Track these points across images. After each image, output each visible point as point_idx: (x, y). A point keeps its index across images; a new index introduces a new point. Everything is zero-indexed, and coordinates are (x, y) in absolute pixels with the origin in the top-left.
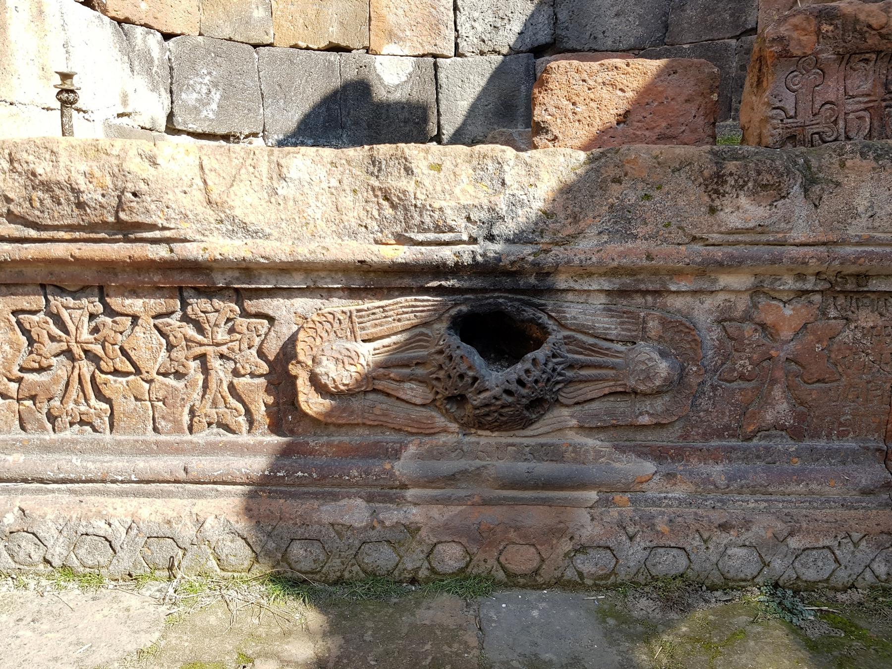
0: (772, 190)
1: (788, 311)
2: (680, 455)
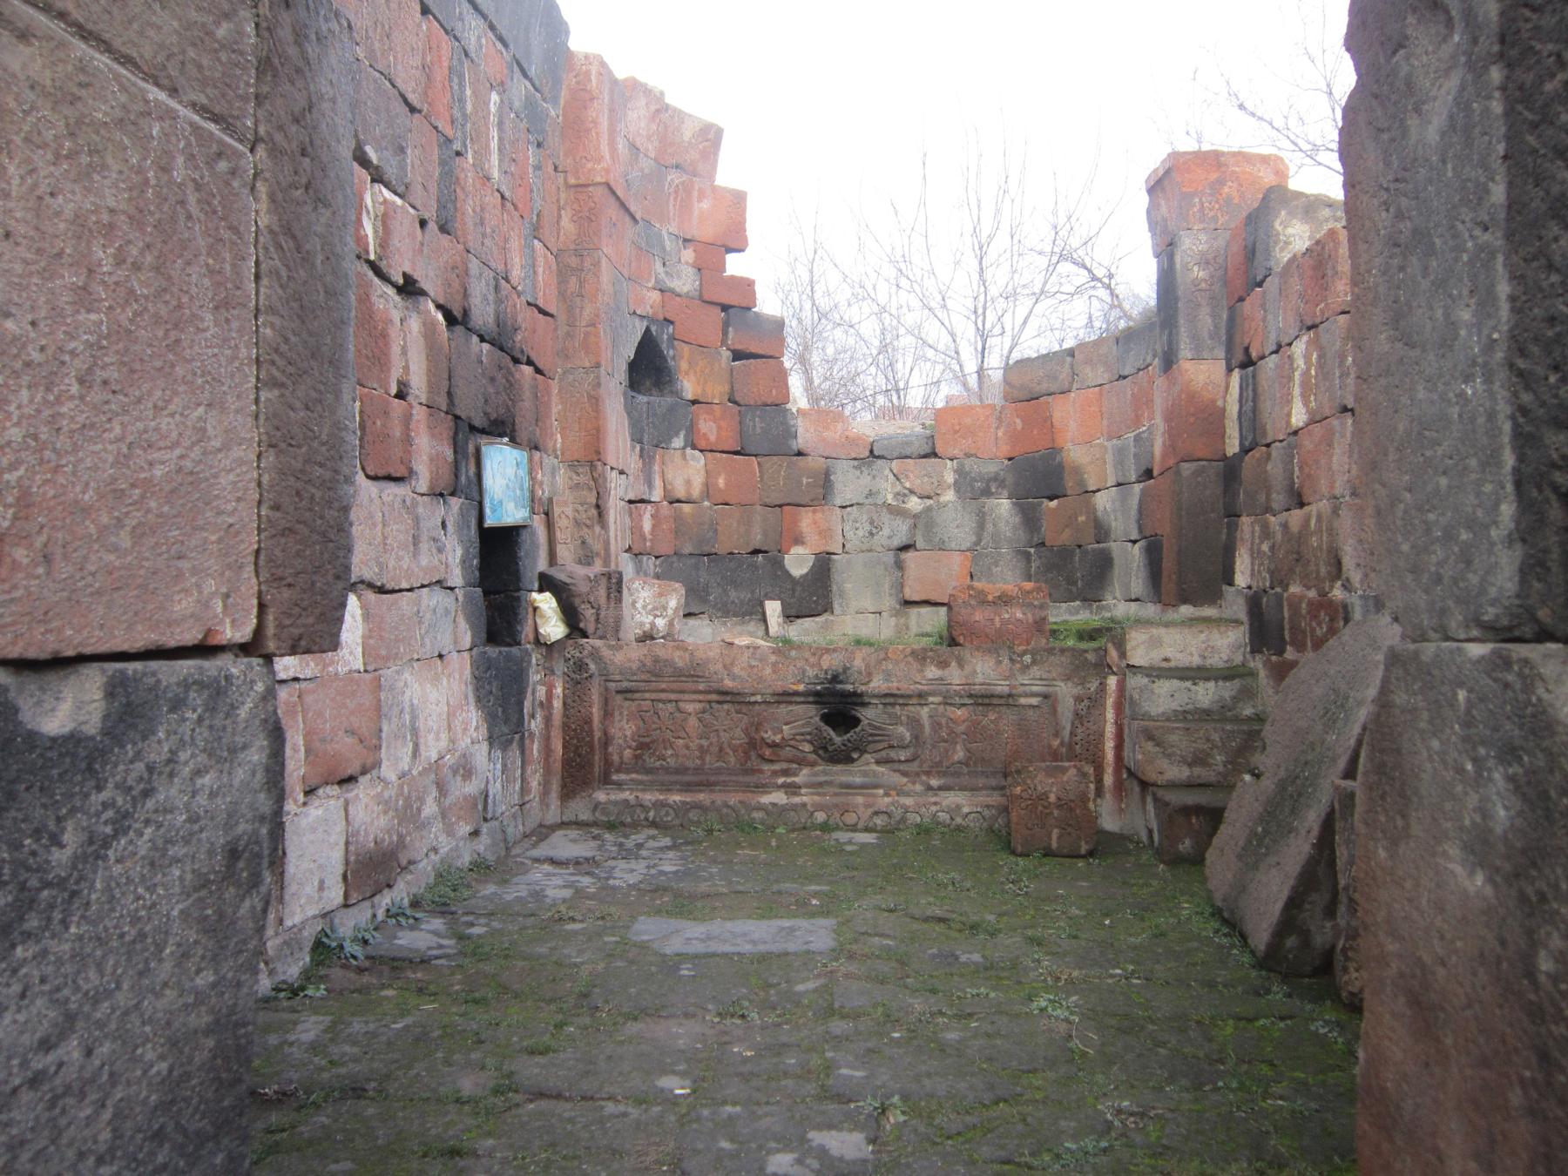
0: (943, 664)
1: (959, 713)
2: (918, 774)
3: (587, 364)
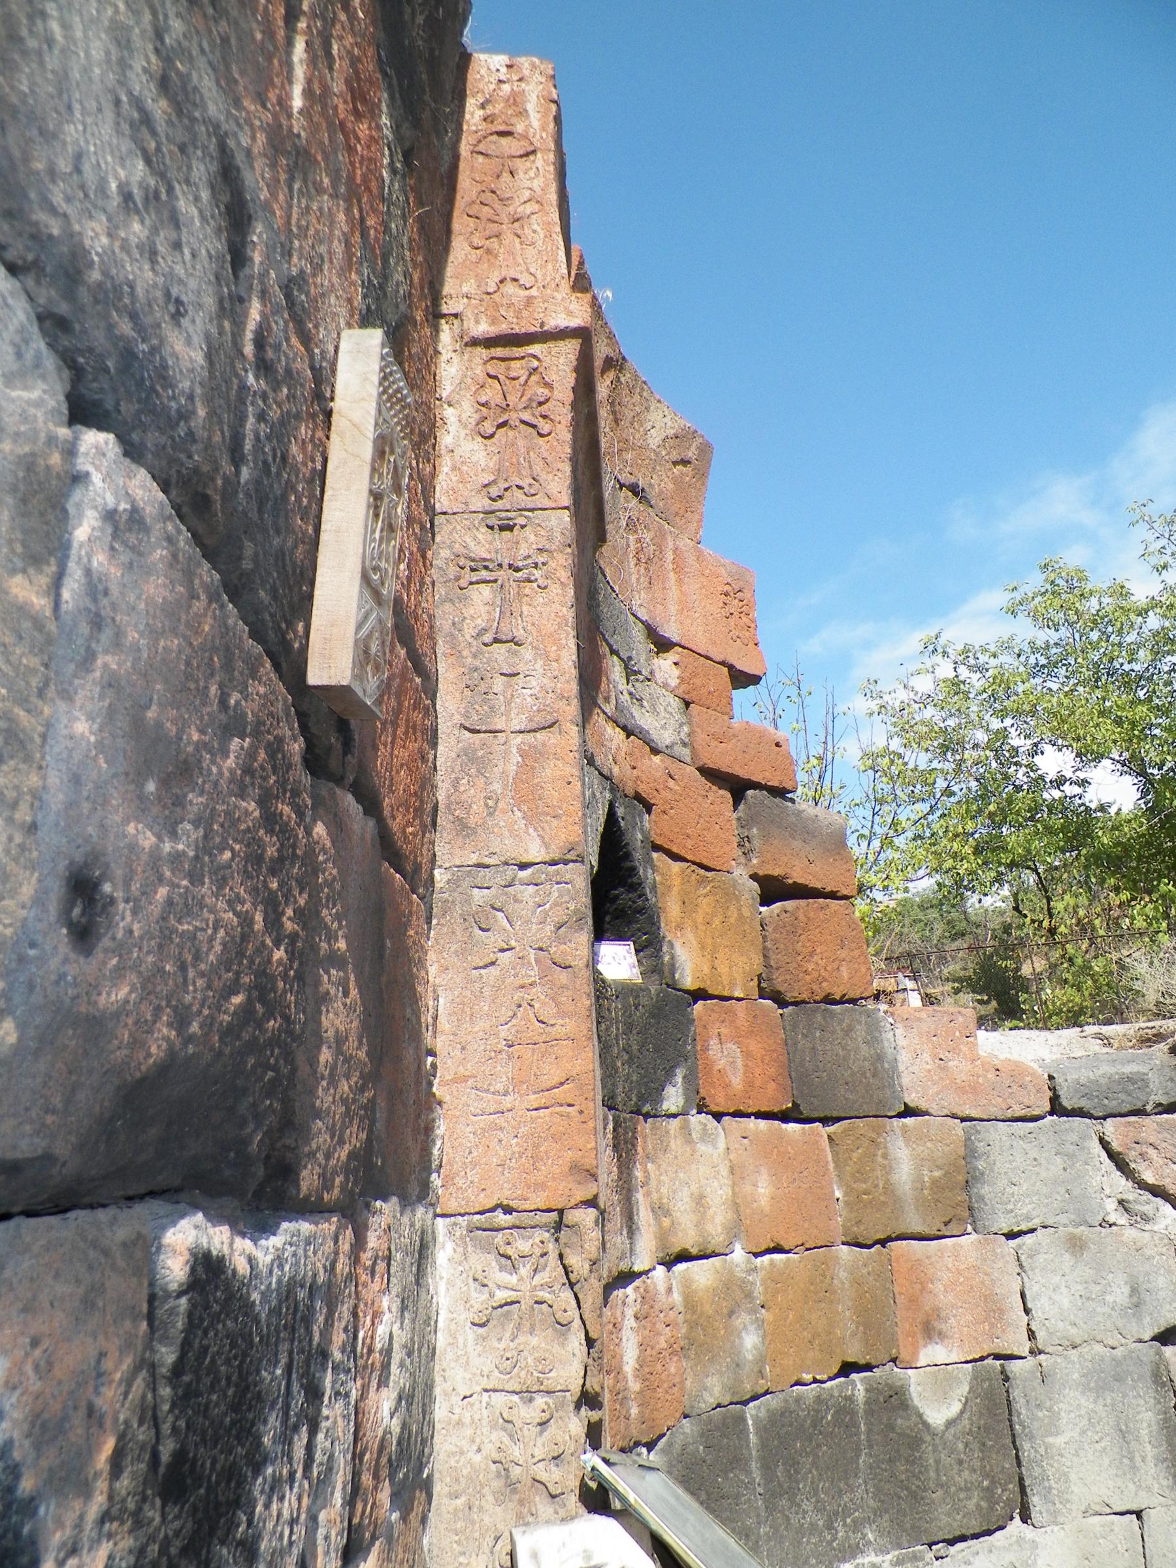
3: (535, 851)
